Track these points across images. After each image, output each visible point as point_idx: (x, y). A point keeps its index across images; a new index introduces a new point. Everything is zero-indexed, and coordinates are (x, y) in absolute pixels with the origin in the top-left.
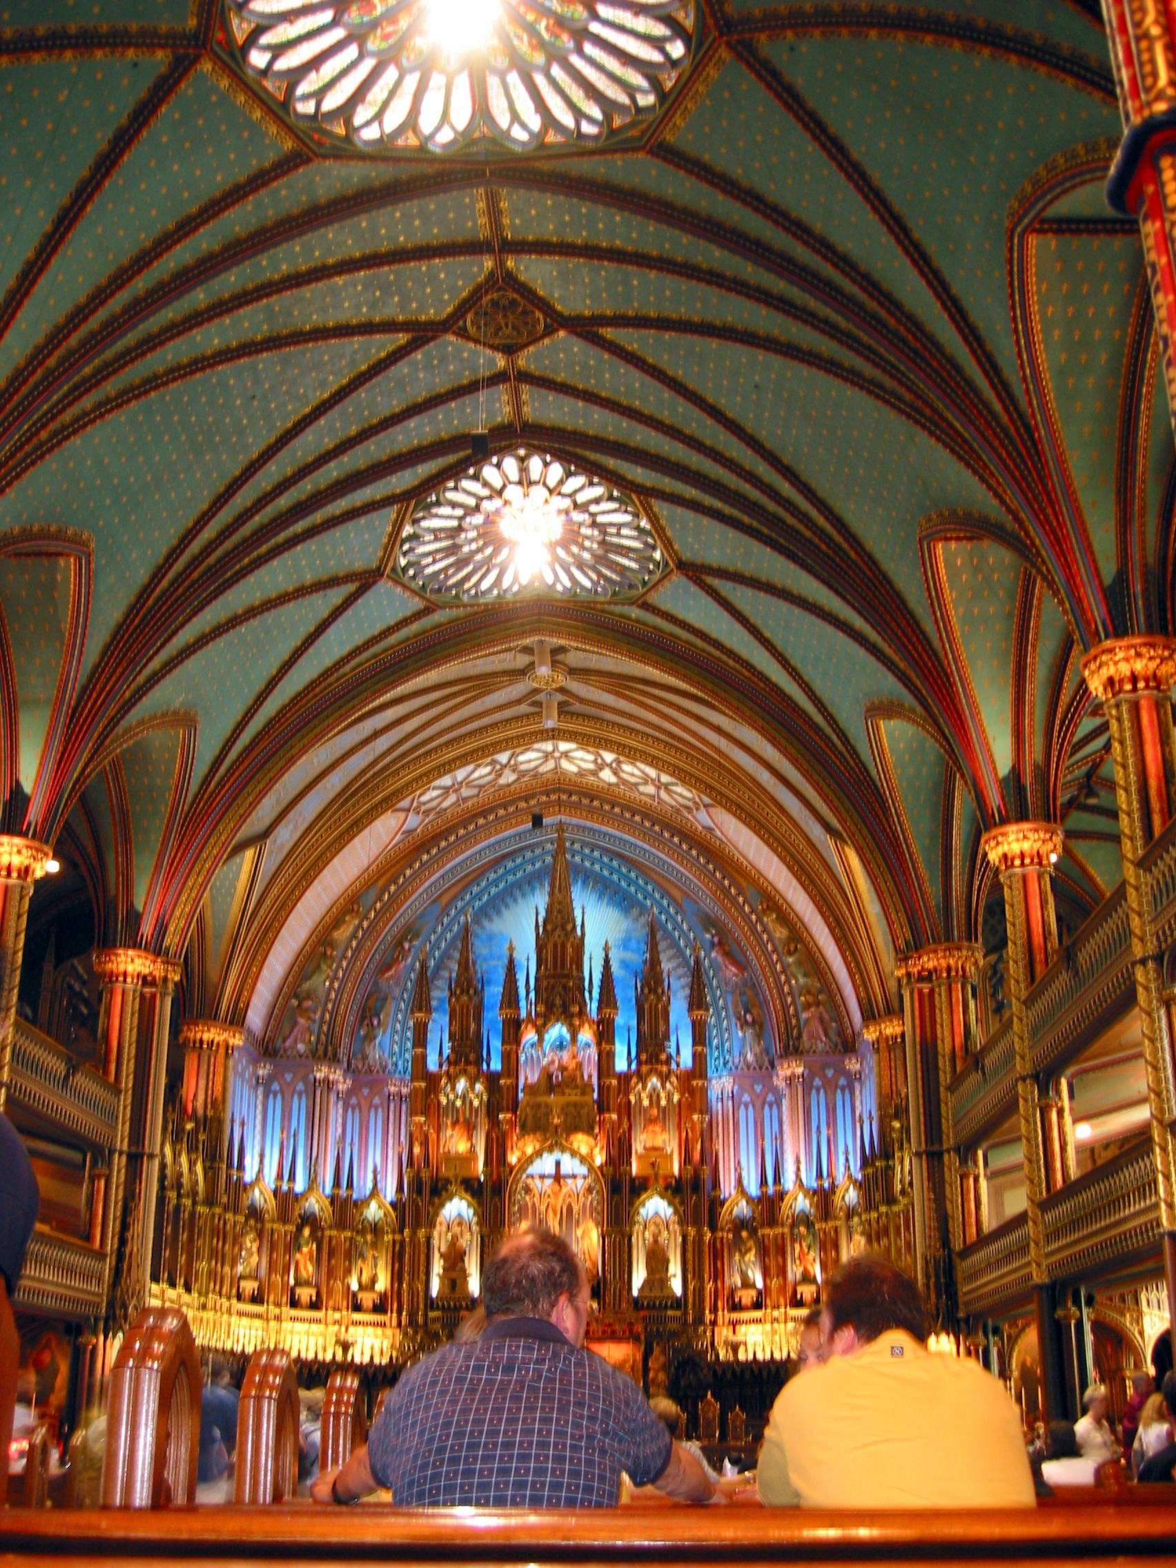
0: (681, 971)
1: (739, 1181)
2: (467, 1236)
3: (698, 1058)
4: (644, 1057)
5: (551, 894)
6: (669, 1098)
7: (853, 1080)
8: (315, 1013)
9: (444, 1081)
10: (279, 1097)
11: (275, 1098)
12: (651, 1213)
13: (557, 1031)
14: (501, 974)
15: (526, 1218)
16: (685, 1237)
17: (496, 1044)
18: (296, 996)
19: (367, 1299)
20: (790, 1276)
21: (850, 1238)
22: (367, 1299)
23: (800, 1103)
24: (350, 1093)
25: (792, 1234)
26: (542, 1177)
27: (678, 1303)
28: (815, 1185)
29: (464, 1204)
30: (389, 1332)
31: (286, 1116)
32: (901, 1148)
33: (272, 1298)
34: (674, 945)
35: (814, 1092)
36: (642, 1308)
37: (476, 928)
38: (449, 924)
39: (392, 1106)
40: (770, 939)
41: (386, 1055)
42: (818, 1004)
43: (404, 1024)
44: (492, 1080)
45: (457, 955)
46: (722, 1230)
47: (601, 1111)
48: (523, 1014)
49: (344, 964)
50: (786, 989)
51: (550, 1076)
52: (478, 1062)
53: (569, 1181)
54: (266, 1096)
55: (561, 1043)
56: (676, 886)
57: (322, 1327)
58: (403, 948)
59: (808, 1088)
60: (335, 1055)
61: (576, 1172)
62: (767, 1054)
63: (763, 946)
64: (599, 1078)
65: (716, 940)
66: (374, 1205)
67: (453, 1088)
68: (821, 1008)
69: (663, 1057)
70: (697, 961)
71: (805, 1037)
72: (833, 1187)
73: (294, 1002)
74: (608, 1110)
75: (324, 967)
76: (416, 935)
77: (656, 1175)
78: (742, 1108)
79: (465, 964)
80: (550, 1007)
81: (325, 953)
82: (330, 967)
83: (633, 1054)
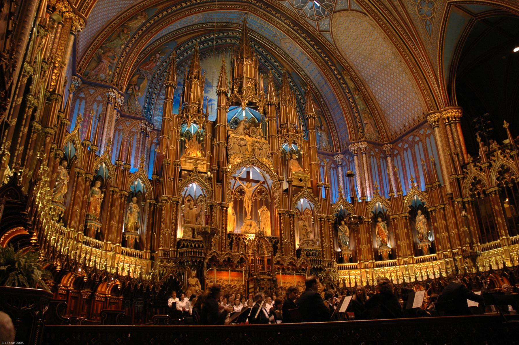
8: (114, 60)
10: (84, 101)
19: (131, 238)
22: (131, 238)
26: (241, 179)
30: (144, 262)
33: (73, 222)
35: (371, 157)
49: (134, 40)
50: (355, 110)
55: (236, 121)
58: (156, 57)
59: (369, 156)
71: (366, 131)
75: (123, 37)
81: (123, 31)
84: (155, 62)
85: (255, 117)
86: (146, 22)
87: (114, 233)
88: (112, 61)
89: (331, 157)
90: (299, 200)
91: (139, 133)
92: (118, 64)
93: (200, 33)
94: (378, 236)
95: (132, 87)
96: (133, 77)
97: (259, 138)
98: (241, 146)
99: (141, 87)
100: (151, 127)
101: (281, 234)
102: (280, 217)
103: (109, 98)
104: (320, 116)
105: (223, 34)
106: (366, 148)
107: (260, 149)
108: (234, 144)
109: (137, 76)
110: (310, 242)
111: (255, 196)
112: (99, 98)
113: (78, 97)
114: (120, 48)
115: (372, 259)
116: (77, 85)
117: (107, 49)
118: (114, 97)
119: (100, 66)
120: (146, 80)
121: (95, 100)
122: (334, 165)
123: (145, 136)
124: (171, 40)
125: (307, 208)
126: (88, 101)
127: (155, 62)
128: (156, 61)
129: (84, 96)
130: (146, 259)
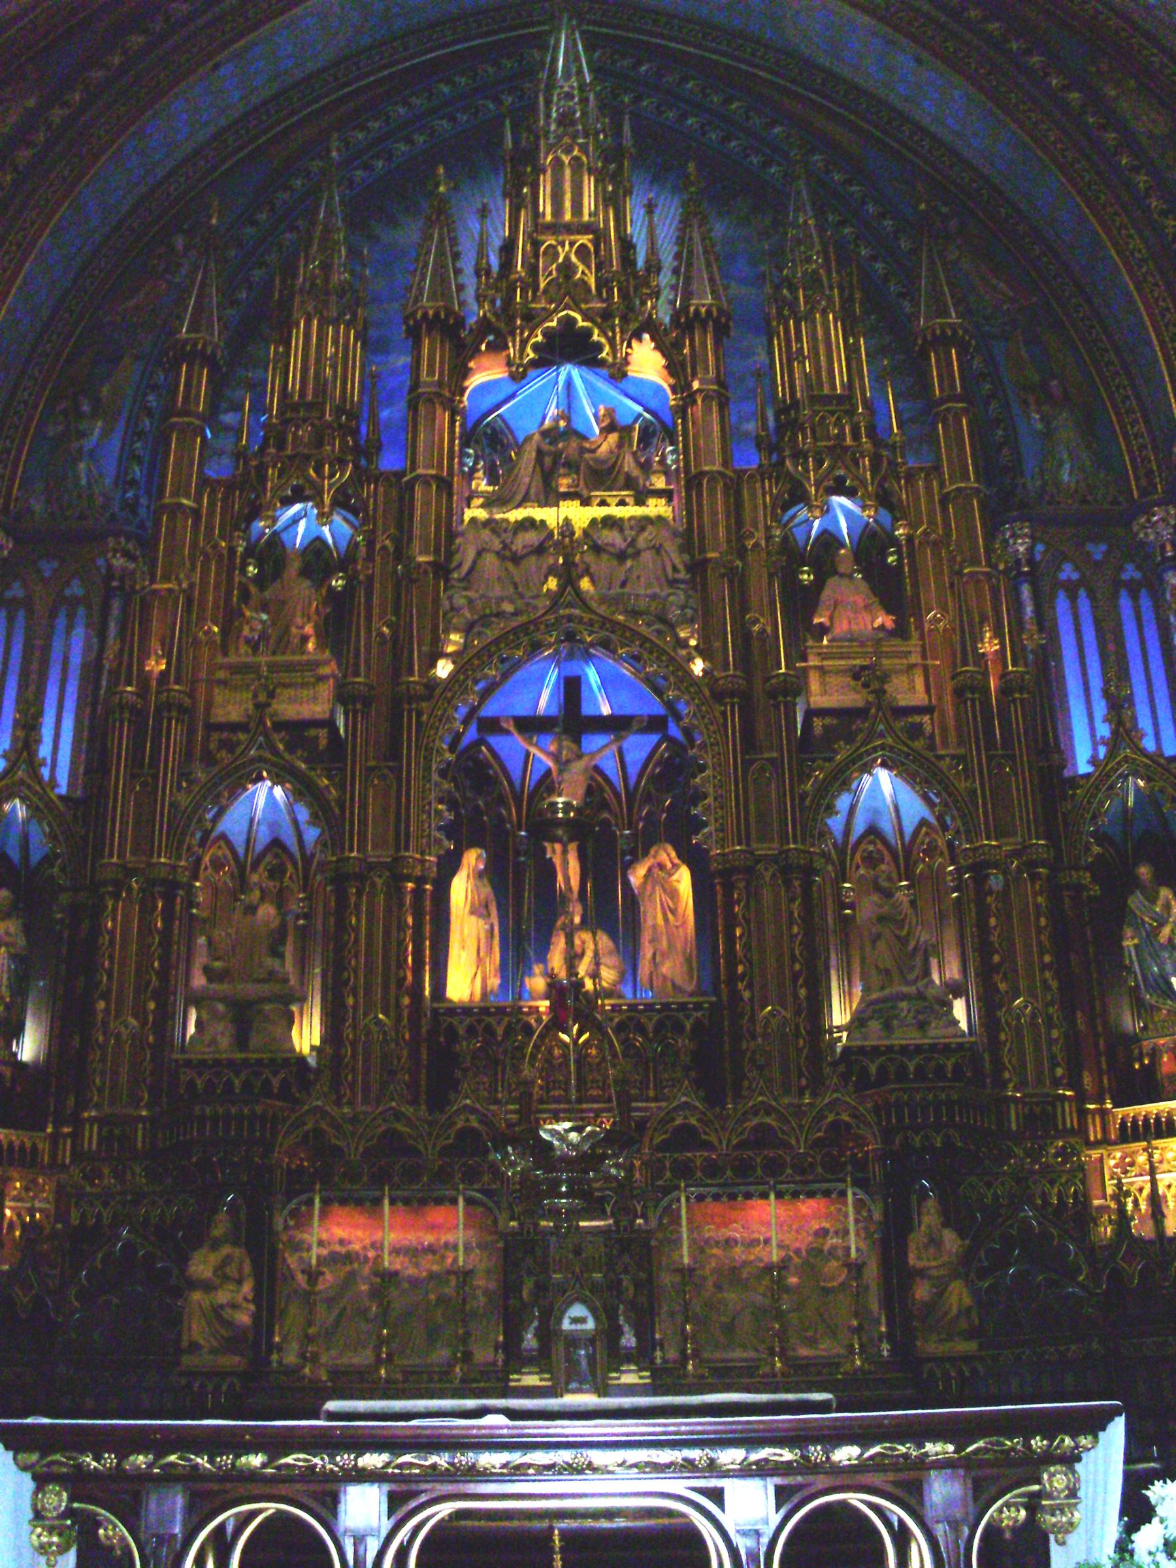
12: (859, 827)
29: (278, 792)
36: (863, 1084)
39: (116, 604)
85: (647, 410)
89: (1120, 531)
90: (845, 785)
91: (96, 601)
97: (622, 503)
98: (516, 559)
107: (621, 556)
108: (479, 554)
110: (904, 1005)
111: (648, 798)
120: (127, 360)
122: (1139, 568)
125: (923, 823)
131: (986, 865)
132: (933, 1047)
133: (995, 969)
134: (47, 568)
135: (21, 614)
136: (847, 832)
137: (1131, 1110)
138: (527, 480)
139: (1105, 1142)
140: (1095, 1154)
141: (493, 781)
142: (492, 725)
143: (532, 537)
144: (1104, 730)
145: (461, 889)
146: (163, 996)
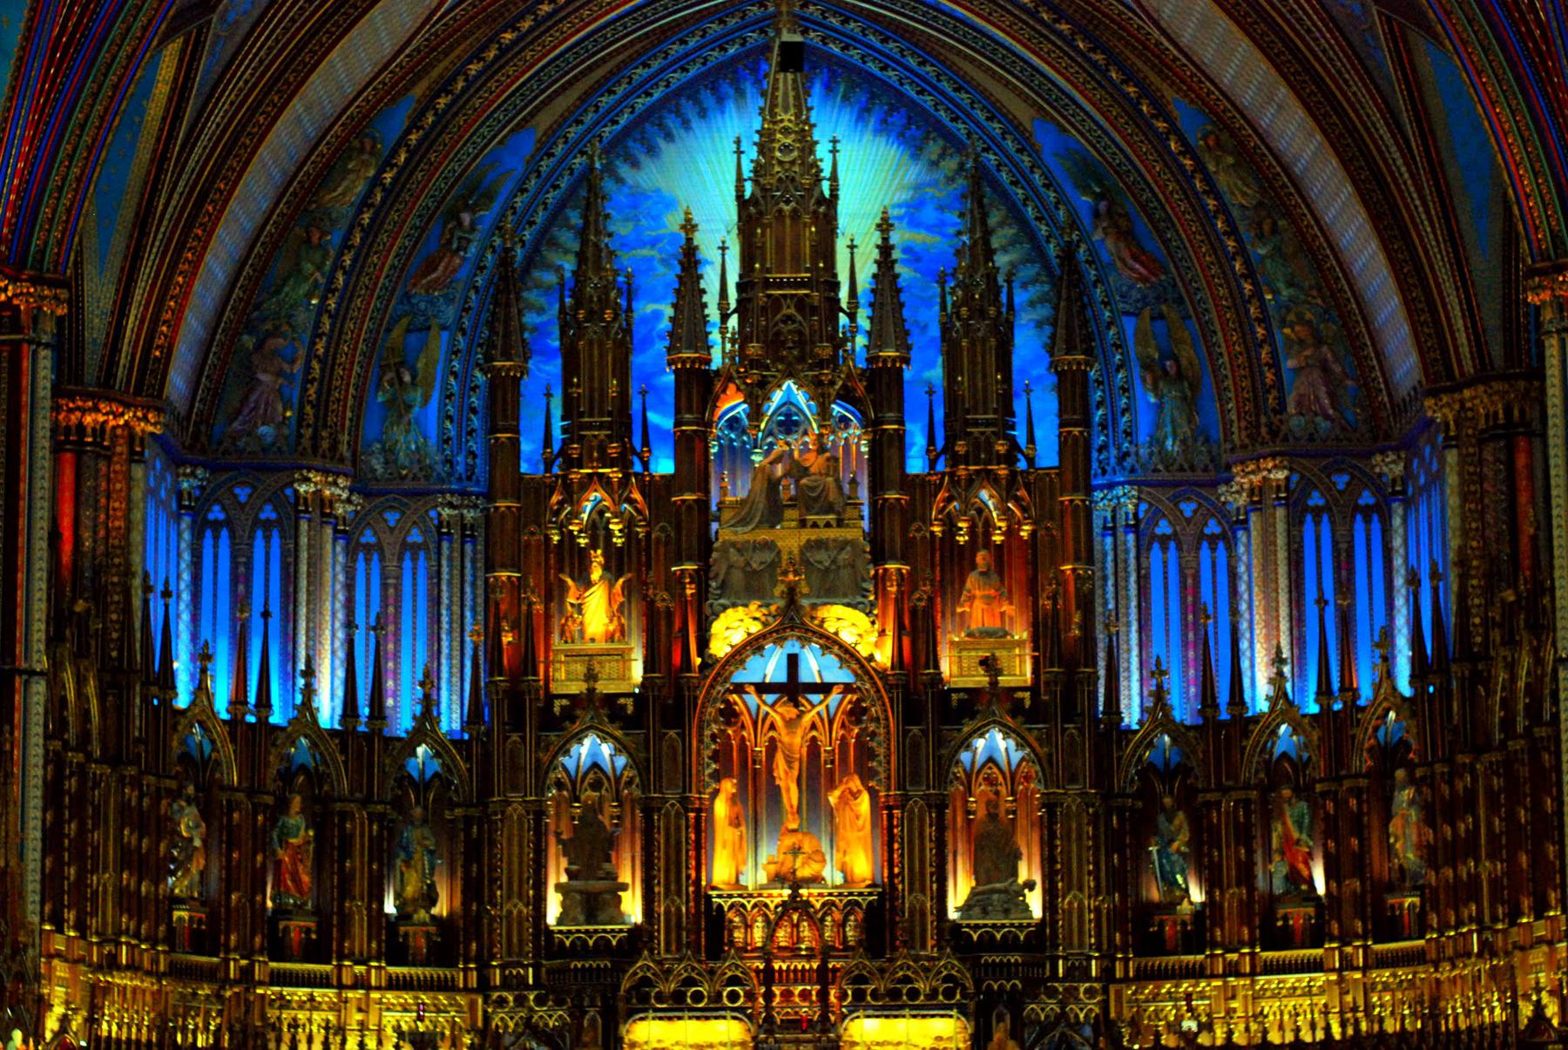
0: (1030, 271)
1: (1160, 695)
2: (611, 808)
3: (1075, 450)
4: (961, 447)
5: (769, 112)
6: (1011, 533)
7: (1388, 497)
8: (292, 362)
9: (555, 498)
10: (225, 533)
11: (216, 538)
12: (980, 759)
13: (789, 393)
14: (668, 274)
15: (730, 776)
16: (1050, 805)
17: (661, 420)
18: (250, 328)
20: (1261, 883)
21: (1387, 817)
23: (1281, 540)
24: (360, 520)
25: (1264, 801)
26: (762, 688)
27: (1041, 939)
28: (1313, 708)
29: (606, 750)
31: (241, 577)
32: (1511, 641)
34: (1015, 215)
35: (1309, 518)
37: (609, 185)
38: (551, 174)
39: (445, 545)
40: (1223, 209)
41: (433, 441)
42: (1319, 341)
43: (464, 378)
44: (658, 490)
45: (568, 239)
46: (1124, 795)
47: (878, 557)
48: (717, 361)
51: (773, 485)
52: (623, 462)
53: (815, 698)
54: (198, 536)
55: (788, 415)
56: (1021, 94)
57: (331, 992)
58: (460, 224)
60: (334, 446)
61: (828, 679)
62: (1207, 441)
63: (1207, 219)
64: (874, 490)
65: (1103, 206)
66: (421, 750)
67: (575, 514)
68: (1325, 349)
69: (1001, 447)
70: (1068, 254)
72: (1352, 706)
73: (248, 341)
74: (894, 558)
75: (308, 267)
76: (489, 197)
77: (994, 684)
78: (1156, 546)
79: (592, 255)
80: (774, 344)
81: (308, 241)
82: (319, 268)
83: (940, 443)
84: (459, 249)
86: (381, 170)
87: (360, 929)
88: (286, 367)
90: (968, 747)
91: (432, 546)
92: (308, 368)
93: (621, 57)
94: (1277, 858)
95: (390, 375)
96: (388, 330)
97: (828, 525)
99: (420, 365)
100: (475, 506)
101: (891, 875)
102: (890, 816)
103: (297, 504)
104: (1164, 308)
105: (722, 21)
106: (1287, 479)
108: (731, 567)
109: (405, 321)
110: (995, 897)
112: (268, 513)
113: (206, 523)
114: (308, 310)
115: (1252, 946)
116: (196, 483)
117: (268, 326)
118: (312, 489)
119: (253, 398)
121: (257, 522)
123: (457, 546)
124: (512, 130)
125: (1023, 759)
126: (239, 532)
127: (459, 249)
128: (464, 244)
129: (221, 516)
130: (466, 990)
131: (1055, 805)
132: (1012, 925)
133: (1057, 872)
134: (392, 517)
135: (375, 557)
136: (973, 763)
137: (1143, 961)
138: (761, 506)
139: (1126, 980)
140: (1118, 986)
141: (736, 715)
142: (740, 689)
143: (768, 557)
144: (1149, 703)
145: (721, 808)
146: (540, 887)
